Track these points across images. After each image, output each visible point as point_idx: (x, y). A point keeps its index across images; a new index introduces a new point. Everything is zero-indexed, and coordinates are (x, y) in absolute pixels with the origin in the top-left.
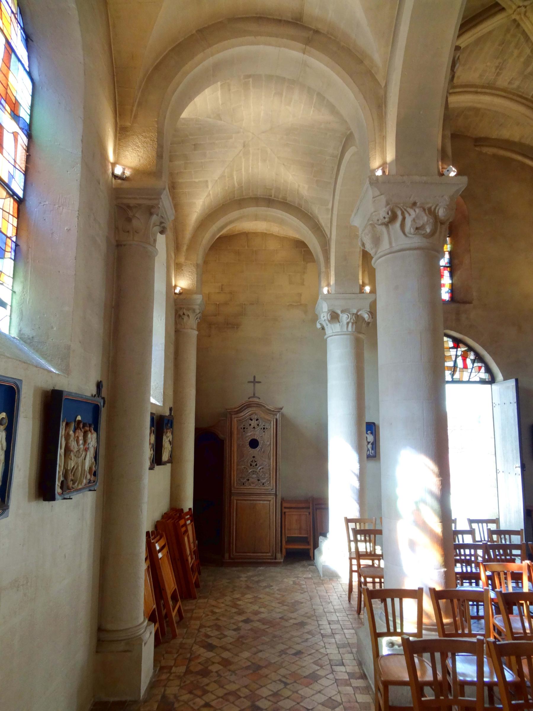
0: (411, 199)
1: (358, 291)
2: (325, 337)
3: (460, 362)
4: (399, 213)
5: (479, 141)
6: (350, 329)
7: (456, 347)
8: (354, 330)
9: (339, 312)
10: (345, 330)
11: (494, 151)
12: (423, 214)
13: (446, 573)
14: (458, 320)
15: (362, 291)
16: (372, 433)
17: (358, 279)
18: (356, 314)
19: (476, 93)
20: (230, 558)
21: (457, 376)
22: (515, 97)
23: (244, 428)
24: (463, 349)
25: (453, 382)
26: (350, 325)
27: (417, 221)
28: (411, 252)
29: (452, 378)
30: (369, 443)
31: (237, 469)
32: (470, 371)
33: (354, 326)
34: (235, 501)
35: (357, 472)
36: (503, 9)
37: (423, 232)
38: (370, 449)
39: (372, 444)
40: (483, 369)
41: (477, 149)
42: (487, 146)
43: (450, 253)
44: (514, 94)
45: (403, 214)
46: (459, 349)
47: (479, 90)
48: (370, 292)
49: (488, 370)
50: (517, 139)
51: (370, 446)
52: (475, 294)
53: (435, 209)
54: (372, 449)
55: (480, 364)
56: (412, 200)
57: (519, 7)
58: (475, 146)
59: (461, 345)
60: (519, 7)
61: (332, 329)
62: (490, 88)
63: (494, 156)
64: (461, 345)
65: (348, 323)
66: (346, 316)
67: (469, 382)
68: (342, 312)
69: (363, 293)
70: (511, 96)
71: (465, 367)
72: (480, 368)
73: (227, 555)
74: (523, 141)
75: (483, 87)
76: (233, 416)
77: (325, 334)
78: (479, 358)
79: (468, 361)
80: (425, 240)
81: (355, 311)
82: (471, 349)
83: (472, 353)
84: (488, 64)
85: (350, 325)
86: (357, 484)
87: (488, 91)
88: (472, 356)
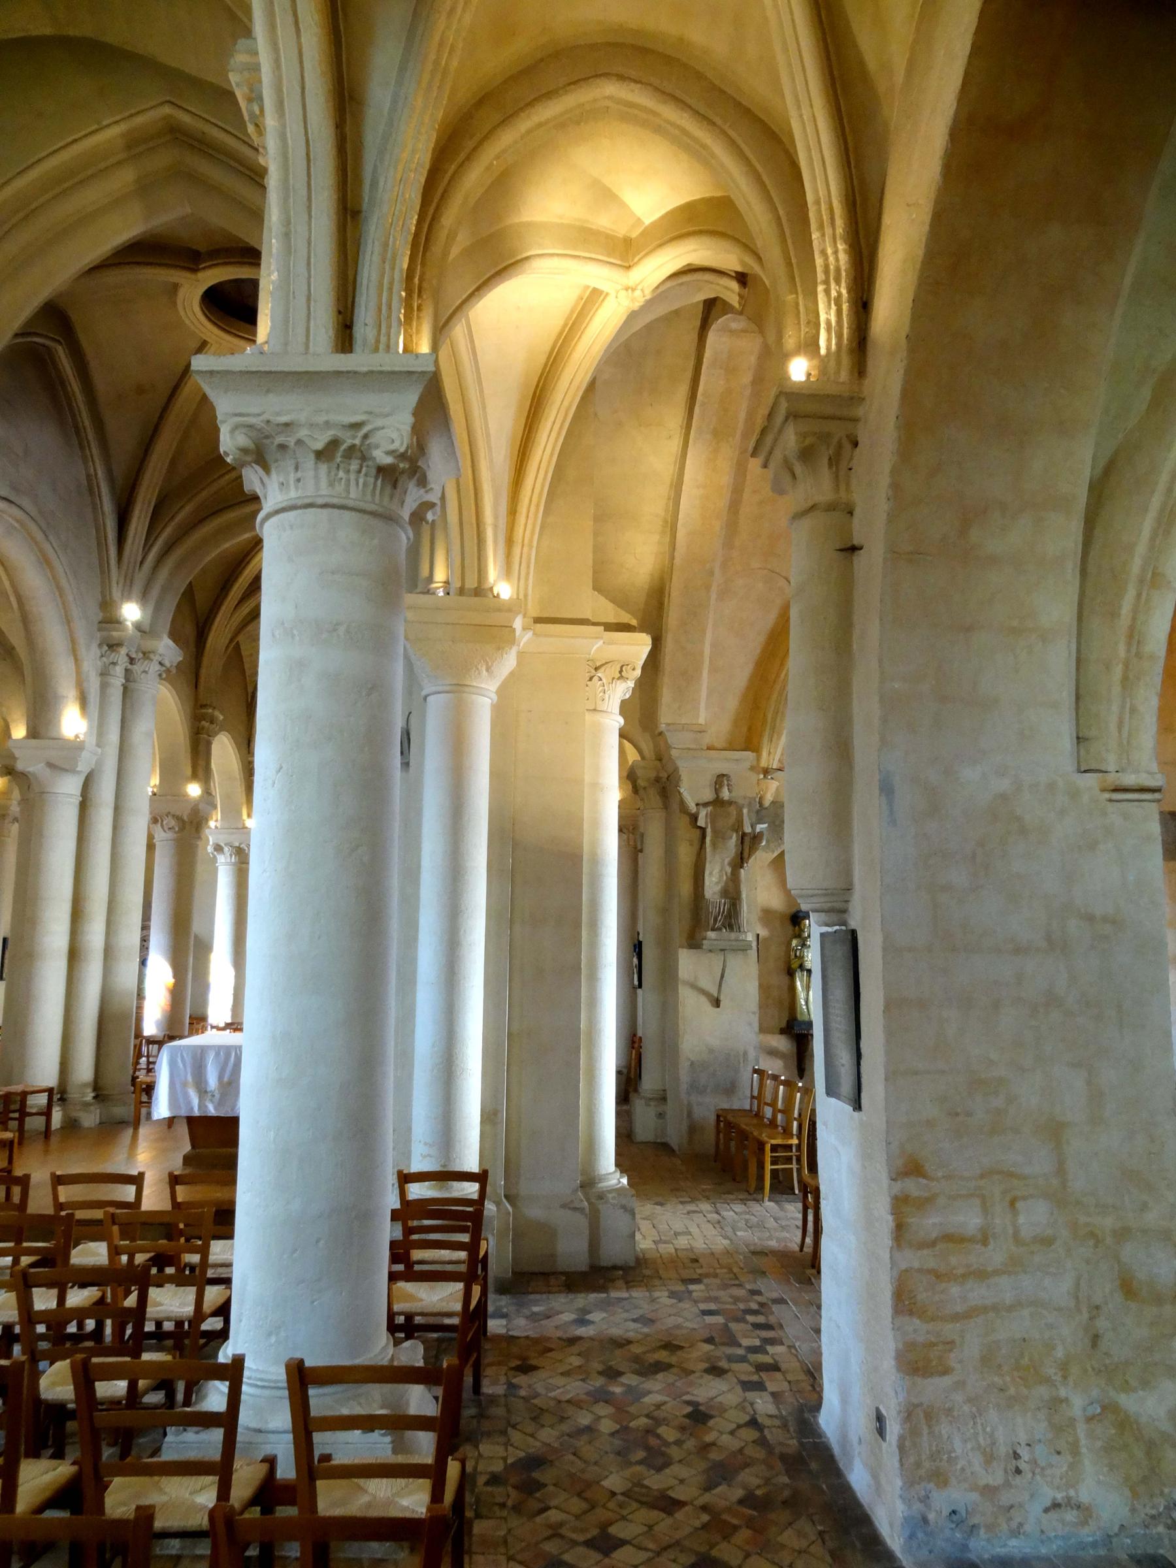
18: (239, 848)
61: (221, 859)
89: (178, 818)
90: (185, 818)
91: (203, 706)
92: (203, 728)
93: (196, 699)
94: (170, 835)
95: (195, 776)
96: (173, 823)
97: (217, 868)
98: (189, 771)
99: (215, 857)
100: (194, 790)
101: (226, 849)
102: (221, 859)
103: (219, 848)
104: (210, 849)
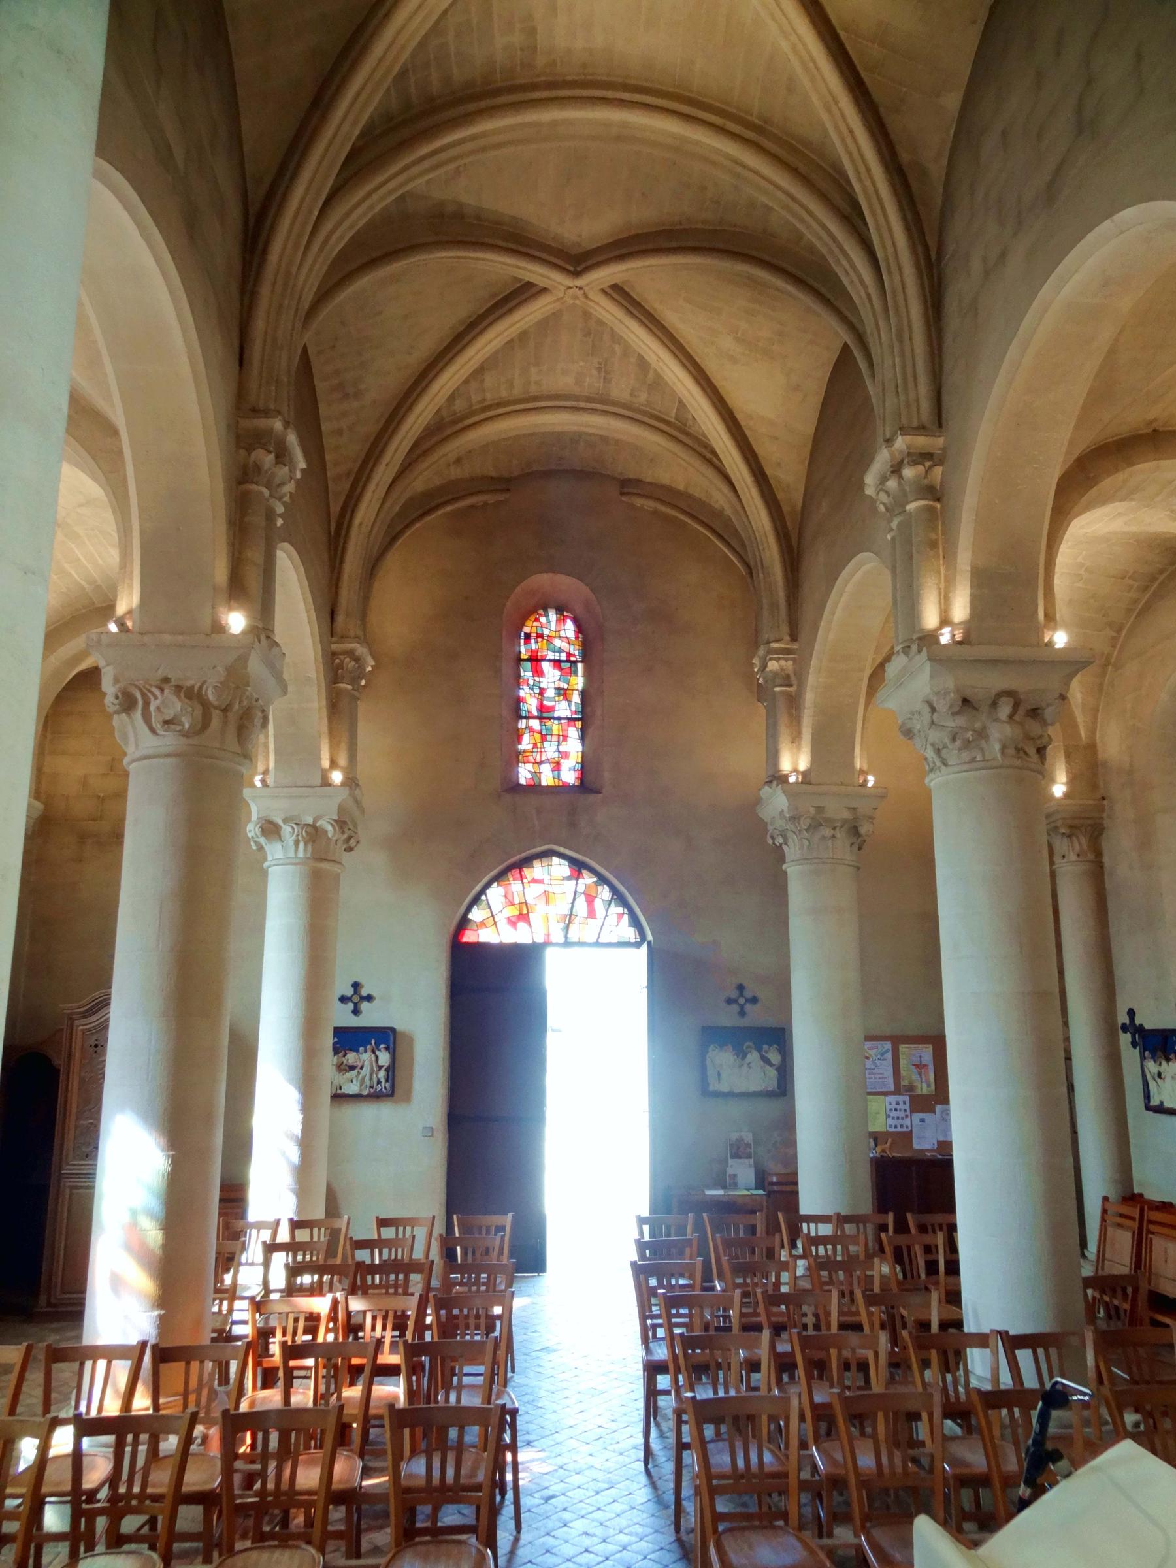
0: (160, 672)
1: (318, 782)
2: (266, 864)
3: (581, 902)
4: (138, 696)
5: (628, 485)
6: (301, 854)
7: (577, 874)
8: (309, 855)
9: (280, 823)
10: (292, 854)
11: (649, 504)
12: (174, 698)
13: (161, 1317)
14: (573, 825)
15: (326, 783)
16: (387, 1049)
17: (320, 759)
18: (313, 826)
19: (577, 409)
20: (49, 1304)
21: (574, 934)
22: (646, 420)
23: (96, 1046)
24: (588, 879)
25: (567, 944)
26: (302, 845)
27: (164, 710)
28: (162, 760)
29: (566, 937)
30: (380, 1067)
31: (76, 1127)
32: (599, 922)
33: (310, 847)
34: (67, 1191)
35: (297, 1129)
36: (545, 290)
37: (179, 728)
38: (383, 1081)
39: (387, 1070)
40: (626, 918)
41: (624, 499)
42: (639, 495)
43: (584, 694)
44: (644, 413)
45: (143, 695)
46: (581, 881)
47: (582, 405)
48: (343, 784)
49: (635, 922)
50: (681, 488)
51: (382, 1074)
52: (607, 775)
53: (201, 687)
54: (387, 1081)
55: (620, 910)
56: (161, 673)
57: (570, 288)
58: (622, 494)
59: (585, 873)
60: (570, 288)
61: (275, 851)
62: (600, 403)
63: (655, 512)
64: (585, 873)
65: (297, 843)
66: (290, 829)
67: (597, 944)
68: (285, 821)
69: (330, 785)
70: (639, 417)
71: (592, 914)
72: (620, 916)
73: (43, 1298)
74: (691, 491)
75: (589, 399)
76: (77, 1023)
77: (265, 859)
78: (618, 897)
79: (598, 905)
80: (183, 740)
81: (310, 820)
82: (603, 880)
83: (606, 888)
84: (582, 363)
85: (302, 845)
86: (294, 1154)
87: (599, 406)
88: (605, 893)
89: (192, 695)
90: (211, 696)
91: (255, 411)
92: (258, 468)
93: (241, 393)
94: (168, 741)
95: (236, 590)
96: (175, 706)
97: (264, 874)
98: (221, 572)
99: (261, 848)
100: (236, 621)
101: (286, 830)
102: (275, 851)
103: (270, 829)
104: (252, 830)
